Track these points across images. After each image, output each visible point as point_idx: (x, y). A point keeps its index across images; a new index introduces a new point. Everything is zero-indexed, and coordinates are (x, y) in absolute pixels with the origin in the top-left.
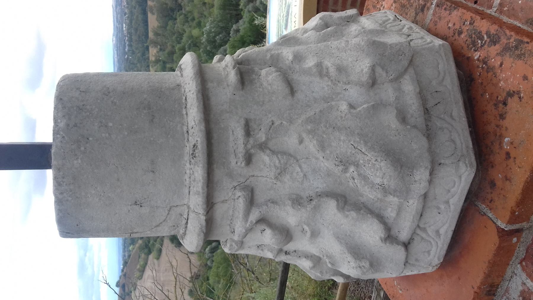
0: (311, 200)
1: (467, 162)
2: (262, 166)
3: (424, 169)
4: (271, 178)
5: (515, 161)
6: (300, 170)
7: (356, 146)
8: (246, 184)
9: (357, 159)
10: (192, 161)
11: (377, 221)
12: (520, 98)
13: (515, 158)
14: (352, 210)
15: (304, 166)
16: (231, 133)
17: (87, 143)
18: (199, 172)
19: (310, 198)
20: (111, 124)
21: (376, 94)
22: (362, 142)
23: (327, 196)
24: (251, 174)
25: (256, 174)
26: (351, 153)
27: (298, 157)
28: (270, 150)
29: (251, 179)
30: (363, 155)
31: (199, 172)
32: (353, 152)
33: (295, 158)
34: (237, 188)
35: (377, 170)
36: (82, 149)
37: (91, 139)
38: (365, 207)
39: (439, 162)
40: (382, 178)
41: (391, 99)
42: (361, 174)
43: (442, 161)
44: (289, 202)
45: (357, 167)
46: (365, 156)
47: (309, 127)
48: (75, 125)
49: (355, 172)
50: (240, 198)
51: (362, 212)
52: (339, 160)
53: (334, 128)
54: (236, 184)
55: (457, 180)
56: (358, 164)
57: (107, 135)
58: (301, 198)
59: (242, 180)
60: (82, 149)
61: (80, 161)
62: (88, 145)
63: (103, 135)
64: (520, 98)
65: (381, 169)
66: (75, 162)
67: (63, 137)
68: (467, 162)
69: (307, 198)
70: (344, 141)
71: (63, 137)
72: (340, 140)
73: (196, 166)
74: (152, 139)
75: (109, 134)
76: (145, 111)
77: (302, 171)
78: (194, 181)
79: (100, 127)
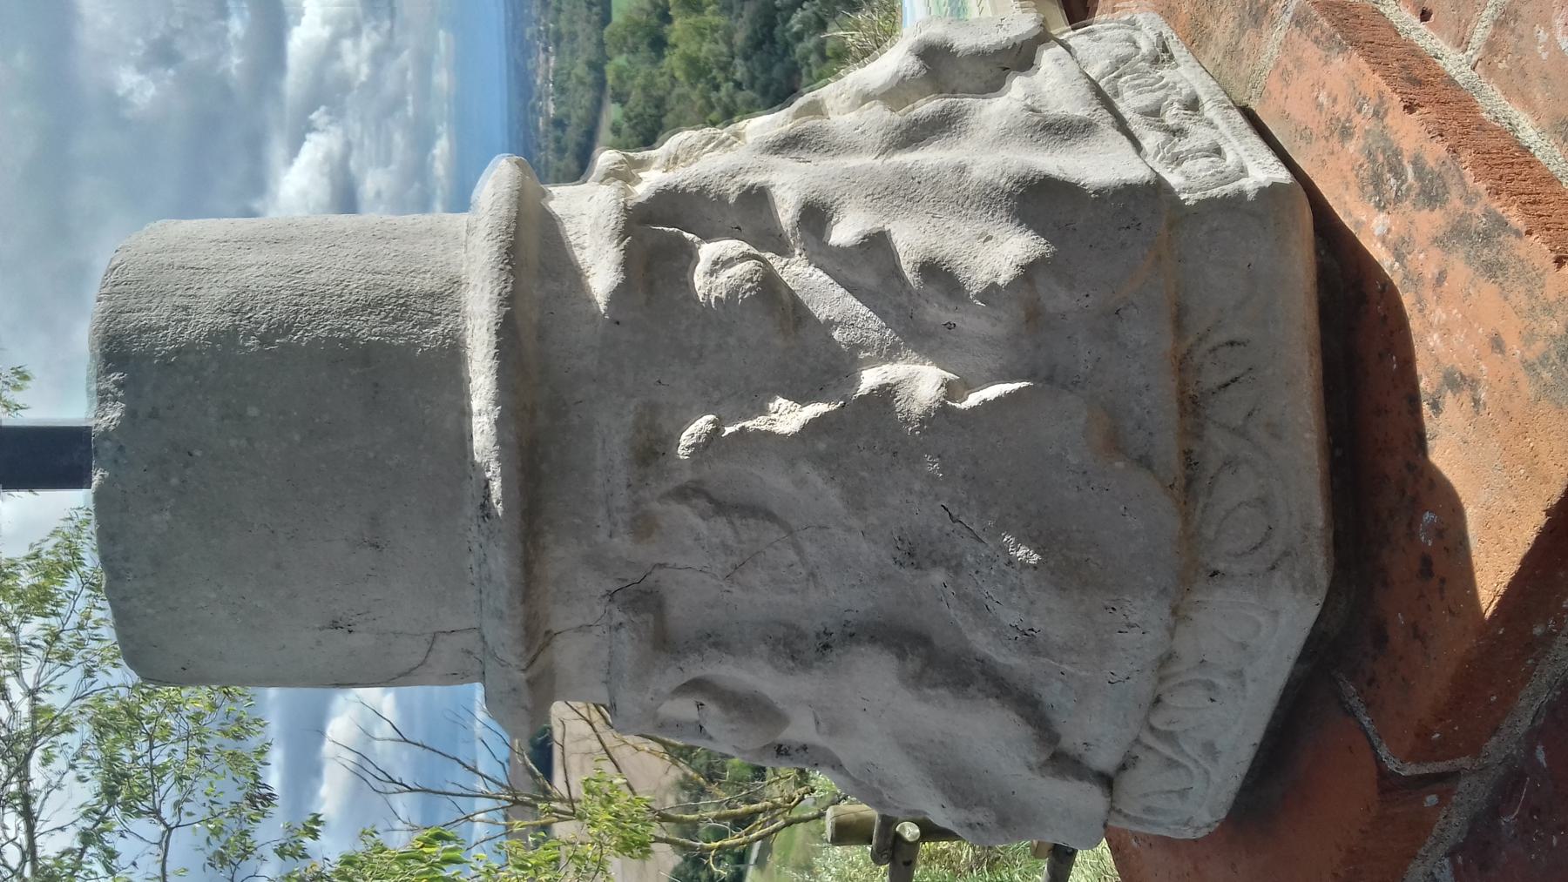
0: (826, 646)
1: (1297, 575)
2: (689, 542)
3: (1154, 593)
4: (714, 576)
5: (1441, 590)
6: (795, 558)
7: (955, 514)
8: (642, 586)
9: (958, 550)
10: (483, 526)
11: (1016, 717)
12: (1476, 402)
13: (1443, 581)
14: (945, 684)
15: (810, 549)
16: (600, 445)
17: (186, 466)
18: (500, 559)
19: (825, 639)
20: (253, 411)
21: (1039, 346)
22: (973, 502)
23: (873, 640)
24: (656, 561)
25: (671, 561)
26: (940, 530)
27: (794, 523)
28: (711, 500)
29: (658, 573)
30: (975, 543)
31: (500, 559)
32: (948, 528)
33: (784, 525)
34: (616, 596)
35: (1012, 589)
36: (174, 481)
37: (198, 453)
38: (983, 673)
39: (1213, 566)
40: (1028, 613)
41: (1082, 369)
42: (966, 595)
43: (1221, 566)
44: (763, 647)
45: (956, 573)
46: (980, 546)
47: (822, 446)
48: (154, 414)
49: (950, 589)
50: (622, 631)
51: (972, 690)
52: (906, 547)
53: (895, 453)
54: (613, 586)
55: (1263, 630)
56: (959, 565)
57: (243, 442)
58: (802, 636)
59: (633, 576)
60: (174, 481)
61: (167, 516)
62: (188, 472)
63: (233, 442)
64: (1476, 402)
65: (1022, 588)
66: (155, 518)
67: (121, 448)
68: (1297, 575)
69: (818, 636)
70: (922, 494)
71: (121, 448)
72: (910, 491)
73: (492, 544)
74: (371, 455)
75: (249, 440)
76: (354, 372)
77: (804, 563)
78: (489, 579)
79: (223, 419)
